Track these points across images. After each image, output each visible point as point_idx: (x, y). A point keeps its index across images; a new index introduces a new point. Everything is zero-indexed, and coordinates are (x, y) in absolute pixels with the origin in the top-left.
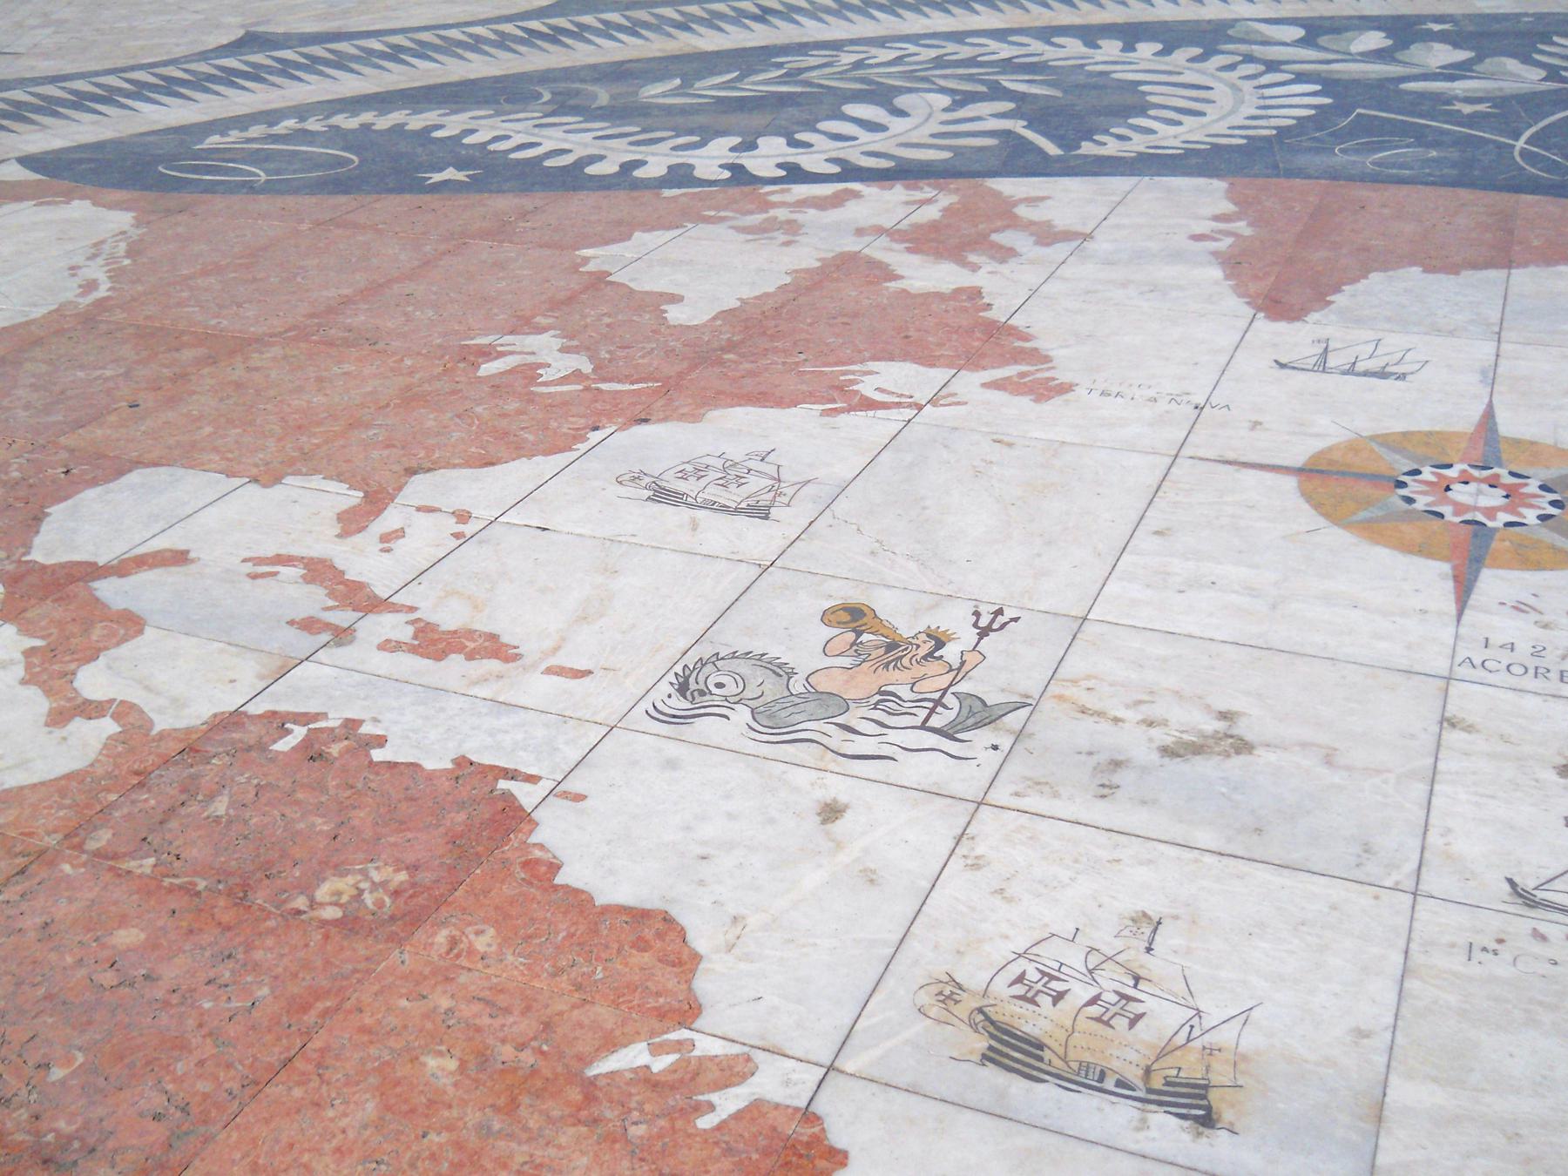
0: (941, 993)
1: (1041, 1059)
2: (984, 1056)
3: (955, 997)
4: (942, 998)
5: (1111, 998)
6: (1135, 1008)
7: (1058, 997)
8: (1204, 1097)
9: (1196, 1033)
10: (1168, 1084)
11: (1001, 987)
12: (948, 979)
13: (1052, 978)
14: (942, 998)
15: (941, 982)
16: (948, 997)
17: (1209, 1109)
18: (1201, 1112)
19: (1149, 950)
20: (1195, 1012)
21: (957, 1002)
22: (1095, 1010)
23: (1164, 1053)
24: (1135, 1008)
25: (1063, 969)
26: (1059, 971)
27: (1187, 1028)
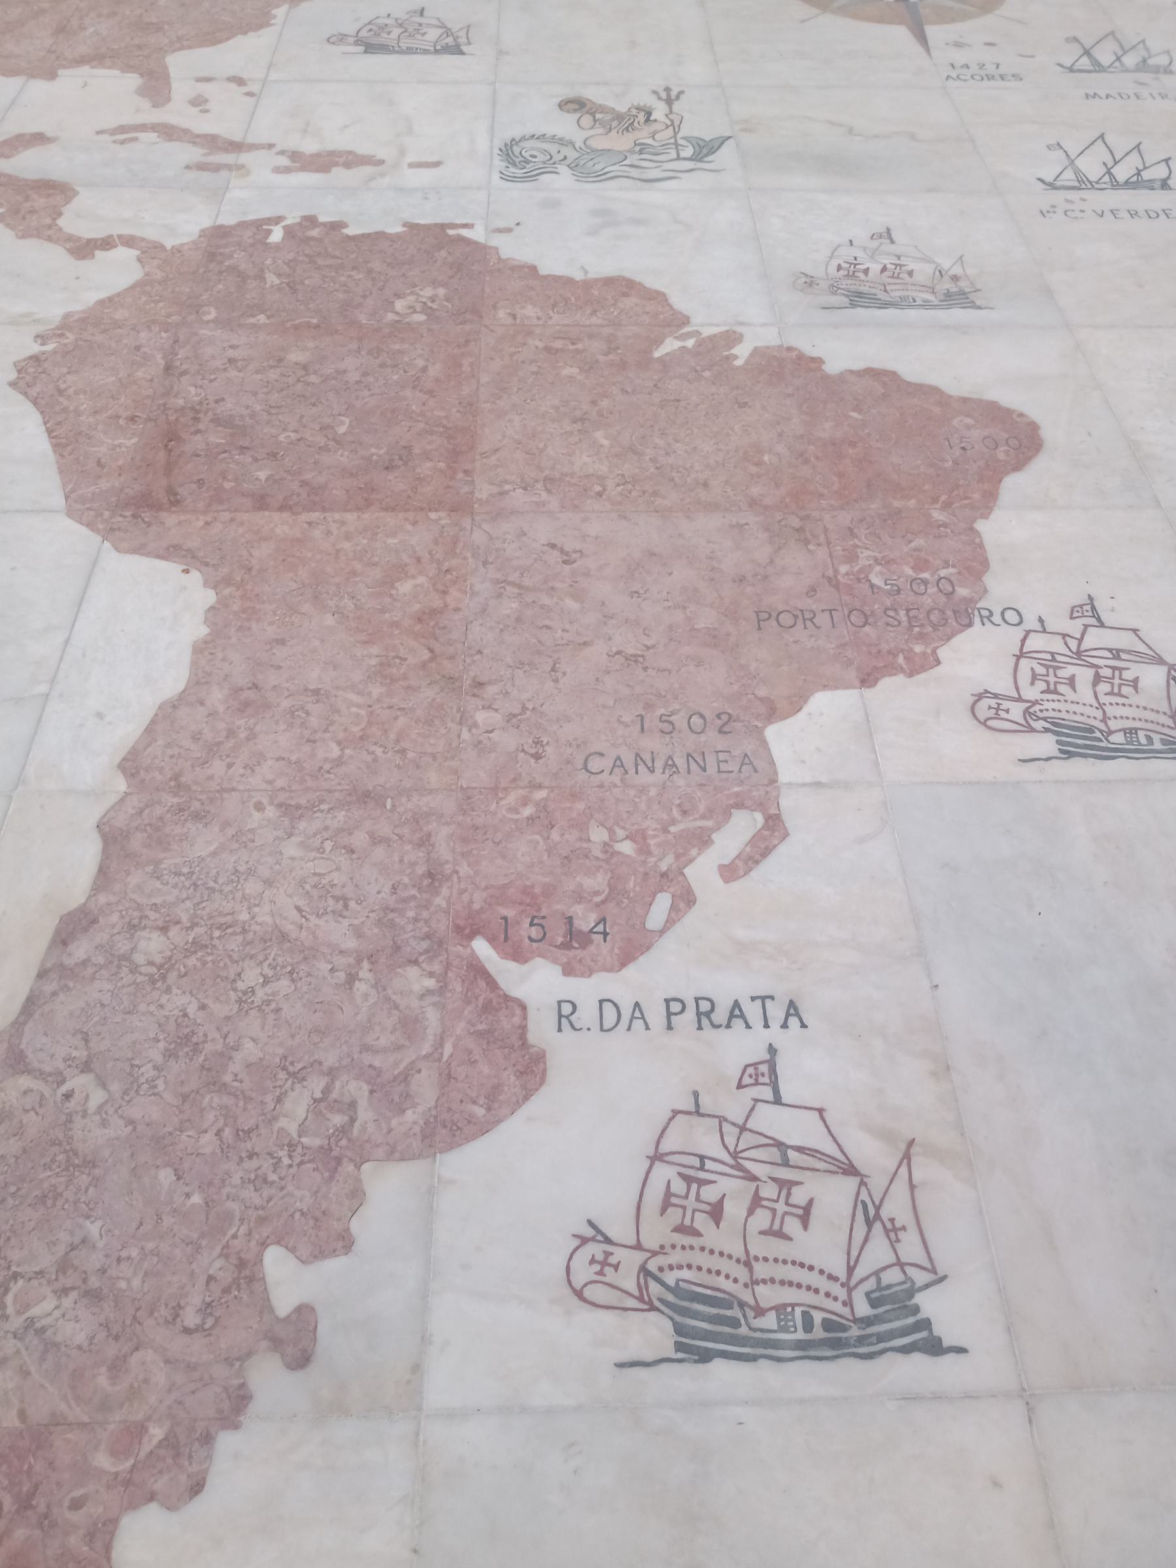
0: (593, 1261)
1: (734, 1323)
2: (679, 1347)
3: (613, 1260)
4: (597, 1267)
5: (769, 1191)
6: (799, 1196)
7: (716, 1212)
8: (916, 1310)
9: (872, 1212)
10: (874, 1304)
11: (656, 1232)
12: (590, 1232)
13: (702, 1182)
14: (597, 1267)
15: (584, 1241)
16: (604, 1263)
17: (926, 1324)
18: (924, 1334)
19: (777, 1100)
20: (858, 1179)
21: (616, 1267)
22: (761, 1219)
23: (854, 1253)
24: (799, 1196)
25: (709, 1165)
26: (702, 1168)
27: (860, 1207)
